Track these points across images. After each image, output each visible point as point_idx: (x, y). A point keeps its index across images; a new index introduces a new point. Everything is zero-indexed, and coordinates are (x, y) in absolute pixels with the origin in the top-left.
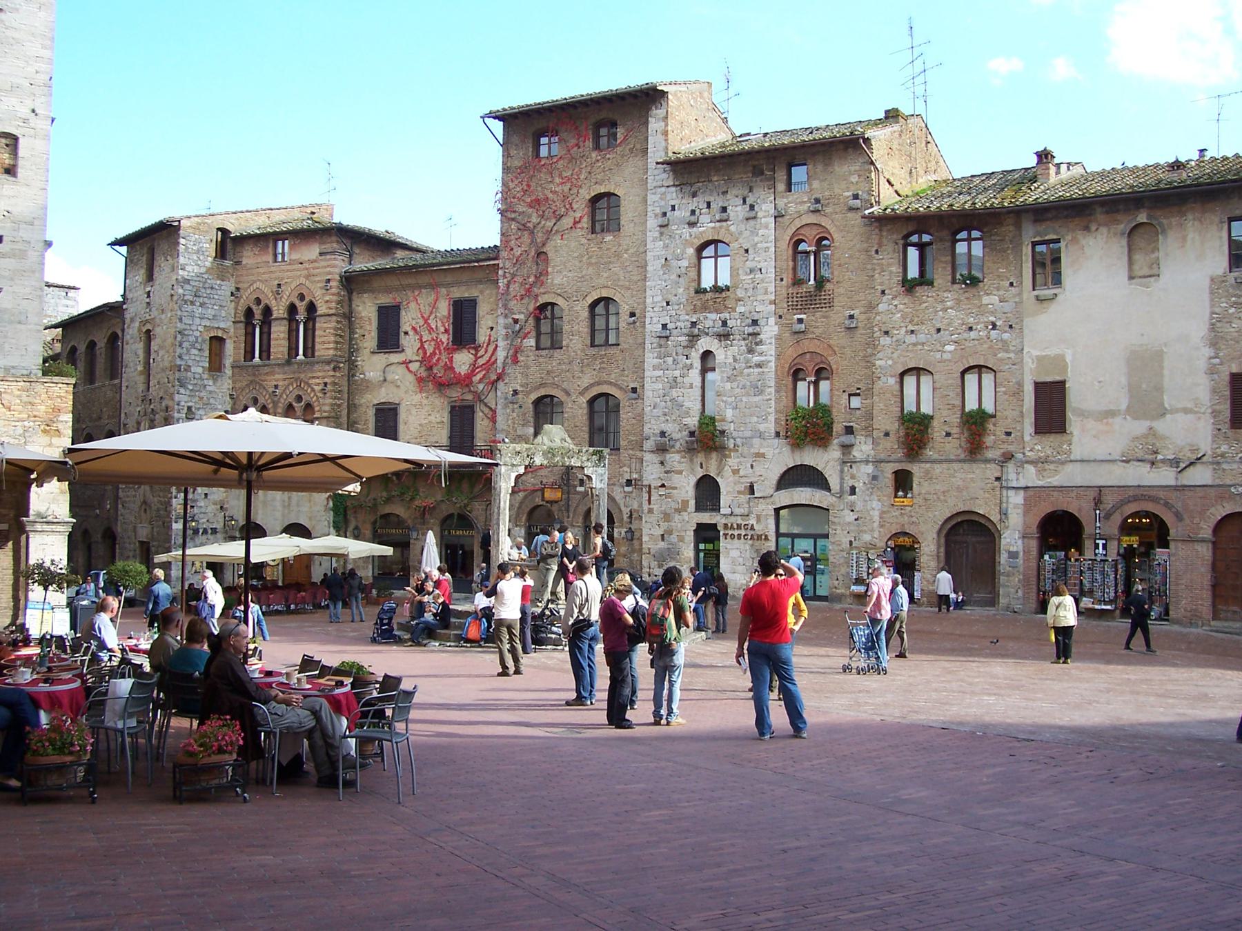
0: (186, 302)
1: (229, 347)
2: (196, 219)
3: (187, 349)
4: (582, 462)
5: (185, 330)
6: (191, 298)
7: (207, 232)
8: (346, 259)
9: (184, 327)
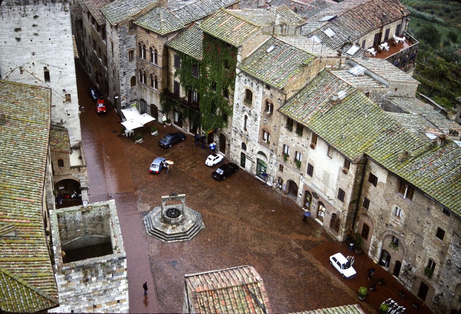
1: (135, 52)
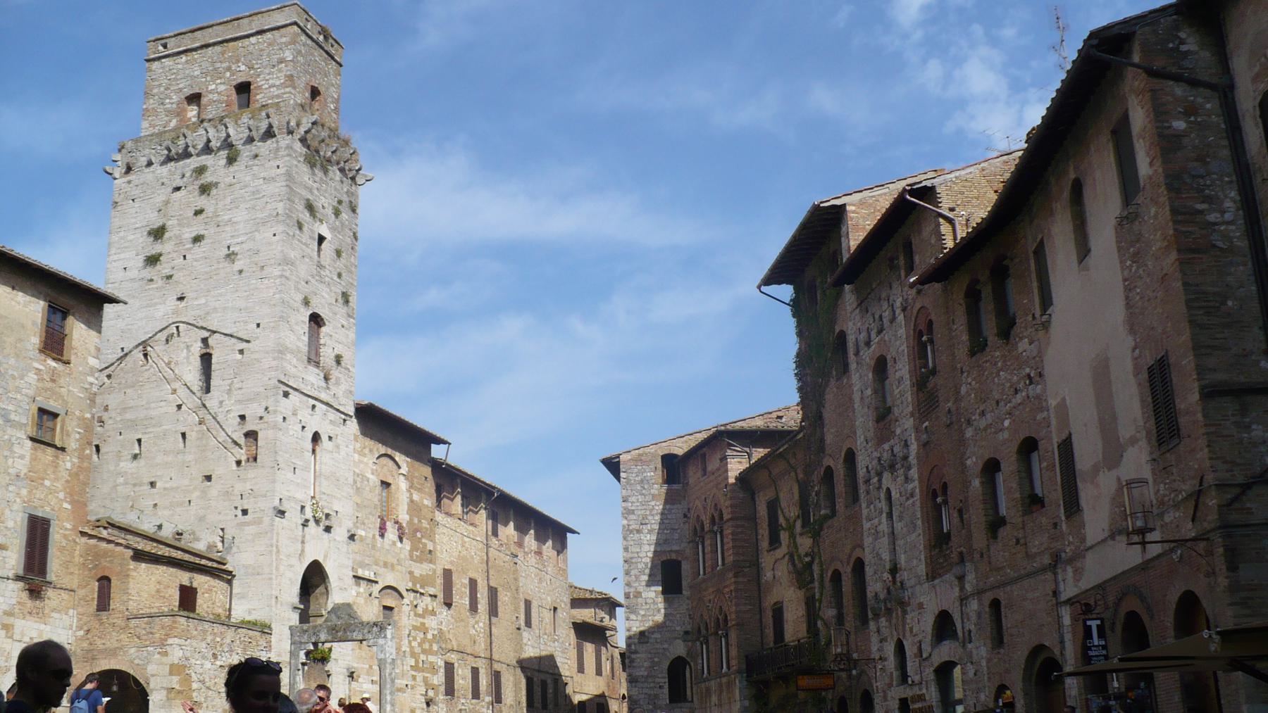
0: (631, 532)
2: (637, 451)
3: (635, 576)
4: (364, 635)
5: (632, 558)
6: (637, 527)
7: (650, 461)
8: (744, 460)
9: (630, 555)
